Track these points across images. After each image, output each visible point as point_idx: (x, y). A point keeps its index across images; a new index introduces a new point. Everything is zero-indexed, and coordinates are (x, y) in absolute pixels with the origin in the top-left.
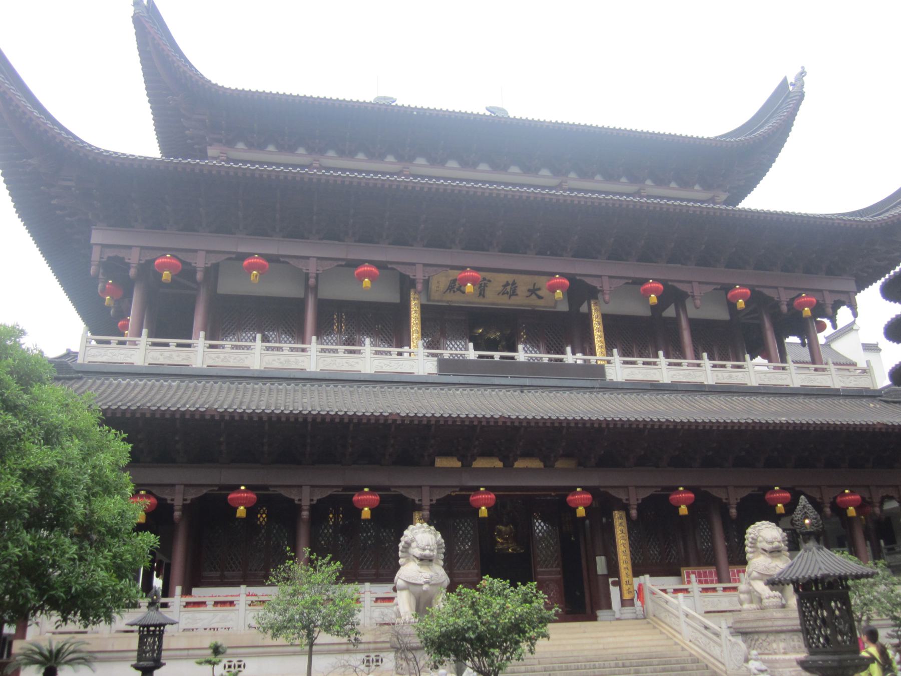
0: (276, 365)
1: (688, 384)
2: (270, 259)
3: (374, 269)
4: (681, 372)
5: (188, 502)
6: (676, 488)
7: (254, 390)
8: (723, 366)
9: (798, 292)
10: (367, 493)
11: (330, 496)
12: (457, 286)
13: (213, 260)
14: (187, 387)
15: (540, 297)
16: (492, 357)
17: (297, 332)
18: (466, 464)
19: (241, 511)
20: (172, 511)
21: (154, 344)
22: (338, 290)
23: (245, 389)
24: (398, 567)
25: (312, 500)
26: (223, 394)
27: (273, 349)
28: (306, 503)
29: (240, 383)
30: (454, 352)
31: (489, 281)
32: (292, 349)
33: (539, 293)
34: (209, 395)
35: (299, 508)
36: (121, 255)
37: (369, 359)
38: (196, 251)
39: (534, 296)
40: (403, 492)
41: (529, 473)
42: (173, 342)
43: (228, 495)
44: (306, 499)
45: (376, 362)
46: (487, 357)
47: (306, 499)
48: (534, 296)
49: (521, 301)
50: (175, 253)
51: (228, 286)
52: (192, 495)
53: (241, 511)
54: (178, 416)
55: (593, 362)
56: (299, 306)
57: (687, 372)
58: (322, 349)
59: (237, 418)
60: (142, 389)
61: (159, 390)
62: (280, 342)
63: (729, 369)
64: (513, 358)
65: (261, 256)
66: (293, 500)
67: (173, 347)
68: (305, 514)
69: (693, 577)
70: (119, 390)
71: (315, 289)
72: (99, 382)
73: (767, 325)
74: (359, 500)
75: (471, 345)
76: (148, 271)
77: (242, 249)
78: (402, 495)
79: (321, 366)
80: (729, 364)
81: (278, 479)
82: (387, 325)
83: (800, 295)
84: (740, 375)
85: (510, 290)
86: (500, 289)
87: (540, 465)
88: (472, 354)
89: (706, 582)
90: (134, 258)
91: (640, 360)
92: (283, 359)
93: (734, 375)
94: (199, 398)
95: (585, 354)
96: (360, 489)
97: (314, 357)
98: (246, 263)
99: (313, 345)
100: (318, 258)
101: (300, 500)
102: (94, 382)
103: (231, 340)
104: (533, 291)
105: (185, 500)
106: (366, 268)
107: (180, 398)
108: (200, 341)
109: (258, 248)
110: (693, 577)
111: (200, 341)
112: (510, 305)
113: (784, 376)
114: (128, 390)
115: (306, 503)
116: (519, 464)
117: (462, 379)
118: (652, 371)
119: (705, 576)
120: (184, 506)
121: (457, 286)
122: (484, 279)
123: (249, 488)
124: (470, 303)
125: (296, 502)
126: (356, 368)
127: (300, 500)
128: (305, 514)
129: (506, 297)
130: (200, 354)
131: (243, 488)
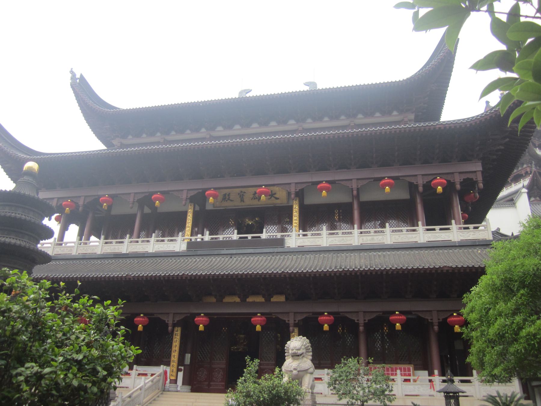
0: (400, 240)
1: (474, 241)
2: (163, 193)
3: (391, 181)
4: (337, 239)
5: (367, 321)
6: (395, 312)
7: (324, 257)
8: (163, 241)
9: (435, 176)
10: (326, 316)
11: (306, 317)
12: (227, 197)
13: (361, 183)
14: (280, 259)
15: (277, 199)
16: (247, 238)
17: (412, 221)
18: (268, 300)
19: (326, 327)
20: (168, 327)
21: (428, 230)
22: (372, 196)
23: (288, 257)
24: (285, 360)
25: (365, 320)
26: (294, 262)
27: (365, 232)
28: (361, 322)
29: (273, 256)
30: (272, 234)
31: (245, 192)
32: (407, 231)
33: (275, 196)
34: (309, 262)
35: (357, 325)
36: (471, 177)
37: (154, 245)
38: (182, 190)
39: (273, 198)
40: (160, 316)
41: (232, 305)
42: (437, 227)
43: (251, 318)
44: (361, 320)
45: (330, 239)
46: (216, 238)
47: (361, 320)
48: (273, 198)
49: (249, 202)
50: (441, 176)
51: (310, 200)
52: (368, 317)
53: (326, 327)
54: (384, 273)
55: (221, 239)
56: (350, 206)
57: (341, 238)
58: (393, 230)
59: (157, 279)
60: (248, 262)
61: (211, 261)
62: (306, 231)
63: (114, 244)
64: (259, 237)
65: (389, 178)
66: (354, 320)
67: (438, 231)
68: (361, 328)
69: (398, 372)
70: (246, 262)
71: (358, 196)
72: (218, 259)
73: (419, 200)
74: (198, 320)
75: (236, 231)
76: (429, 188)
77: (315, 179)
78: (159, 318)
79: (361, 242)
80: (166, 239)
81: (345, 308)
82: (170, 225)
83: (436, 178)
84: (380, 237)
85: (226, 198)
86: (252, 196)
87: (263, 300)
88: (207, 237)
89: (405, 375)
90: (420, 182)
91: (114, 241)
92: (112, 247)
93: (375, 237)
94: (322, 263)
95: (304, 231)
96: (255, 314)
97: (354, 237)
98: (319, 186)
99: (356, 231)
100: (423, 175)
101: (288, 321)
102: (216, 260)
103: (222, 234)
104: (272, 195)
105: (365, 320)
106: (386, 180)
107: (280, 266)
108: (421, 228)
109: (323, 177)
110: (398, 372)
111: (421, 228)
112: (261, 205)
113: (414, 236)
114: (246, 262)
115: (361, 322)
116: (250, 299)
117: (271, 250)
118: (317, 239)
119: (388, 370)
120: (365, 323)
121: (227, 197)
122: (242, 192)
123: (330, 313)
124: (235, 206)
125: (356, 321)
126: (318, 243)
127: (358, 320)
128: (361, 328)
129: (256, 201)
130: (126, 246)
131: (326, 314)
